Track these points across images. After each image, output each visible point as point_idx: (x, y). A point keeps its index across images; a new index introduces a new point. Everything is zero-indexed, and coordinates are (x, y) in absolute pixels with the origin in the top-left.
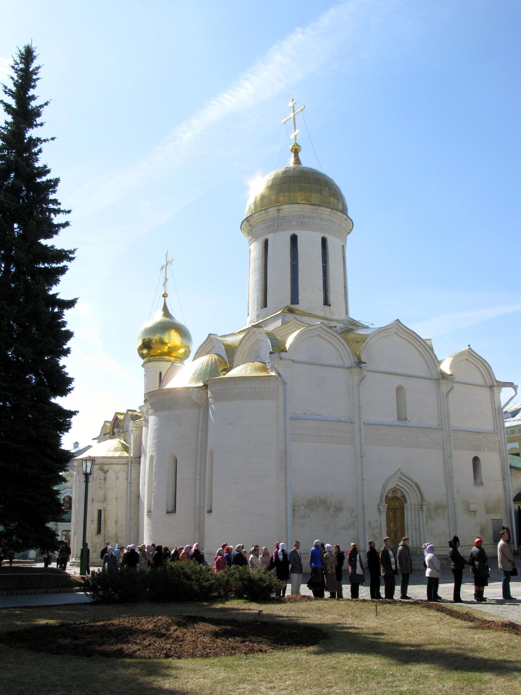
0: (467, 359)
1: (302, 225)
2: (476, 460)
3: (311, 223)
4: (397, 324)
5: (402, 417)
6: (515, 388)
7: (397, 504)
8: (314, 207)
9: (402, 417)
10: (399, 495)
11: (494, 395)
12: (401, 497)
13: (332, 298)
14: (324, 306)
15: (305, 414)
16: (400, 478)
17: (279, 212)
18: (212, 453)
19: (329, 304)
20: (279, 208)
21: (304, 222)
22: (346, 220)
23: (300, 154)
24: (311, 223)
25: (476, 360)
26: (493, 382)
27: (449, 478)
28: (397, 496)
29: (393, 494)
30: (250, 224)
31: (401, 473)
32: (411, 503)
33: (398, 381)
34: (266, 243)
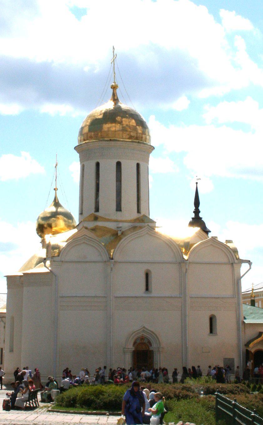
4: (148, 227)
7: (144, 347)
10: (146, 341)
14: (116, 212)
28: (144, 342)
29: (141, 340)
31: (144, 327)
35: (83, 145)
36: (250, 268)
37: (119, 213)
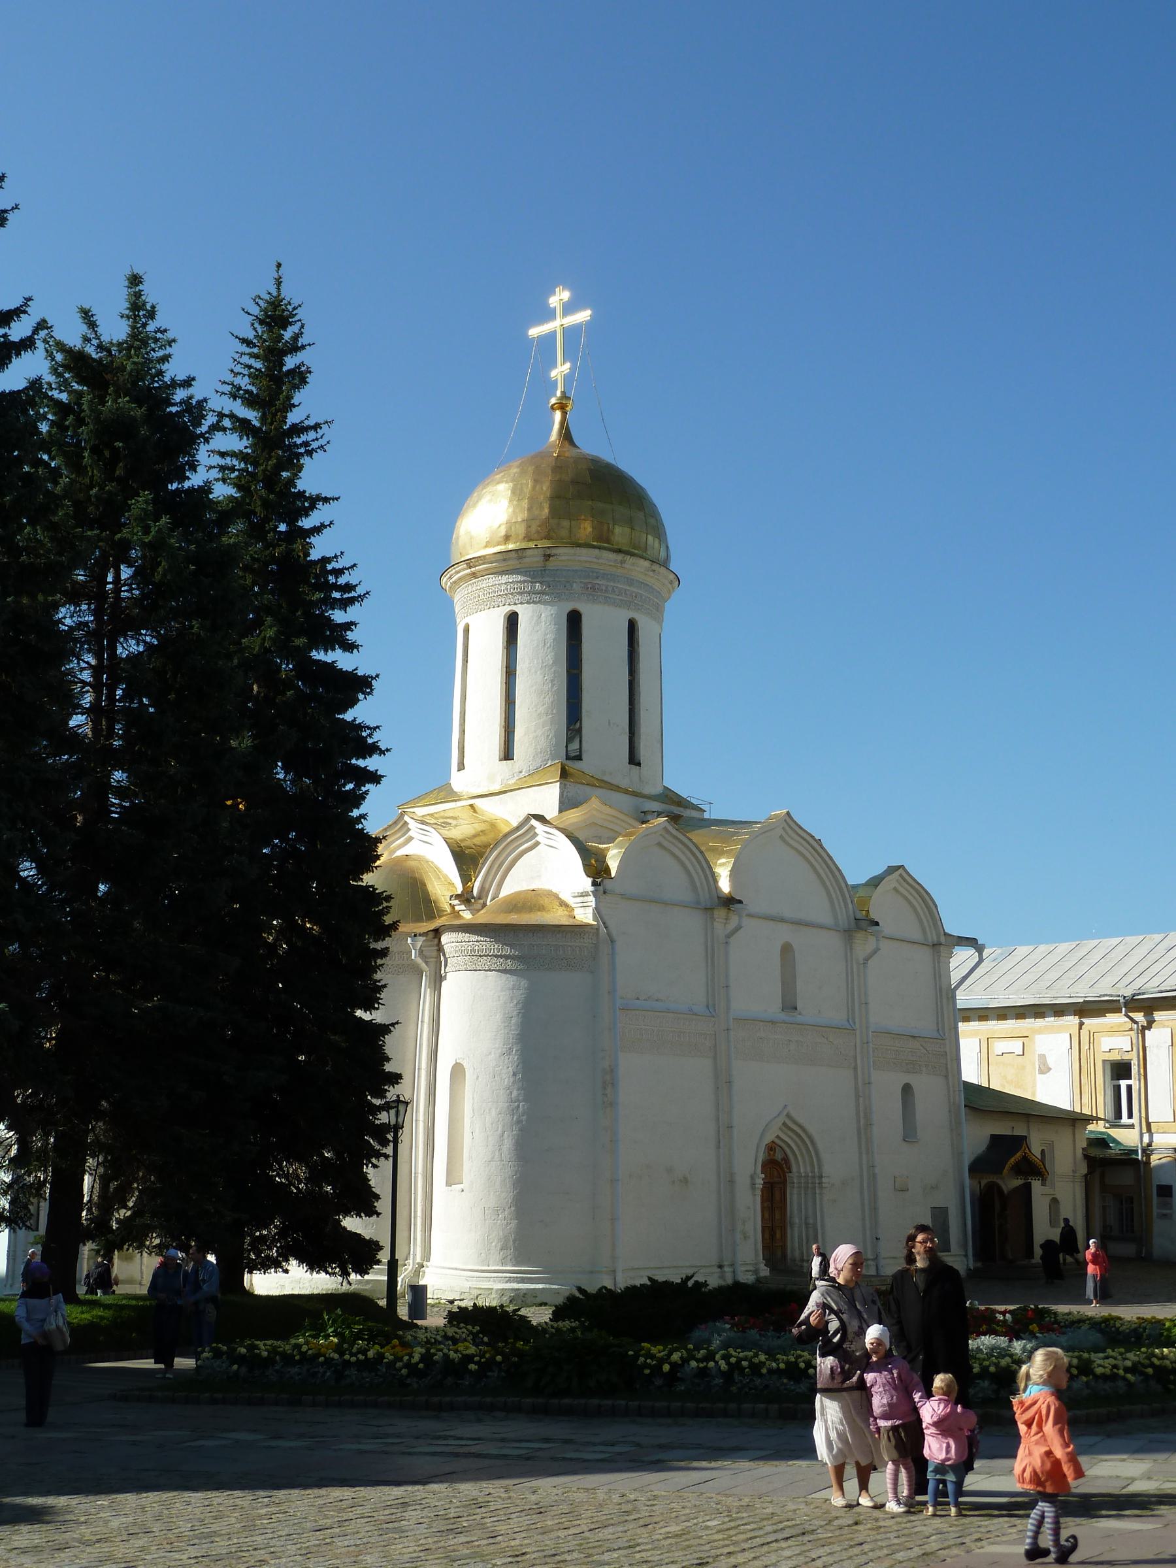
0: (895, 889)
1: (593, 592)
2: (907, 1089)
3: (610, 589)
5: (790, 1006)
6: (980, 949)
7: (776, 1173)
8: (620, 557)
9: (790, 1006)
10: (779, 1156)
11: (939, 962)
12: (782, 1160)
15: (638, 999)
16: (784, 1124)
17: (546, 560)
19: (637, 761)
20: (548, 552)
21: (597, 587)
22: (671, 583)
24: (610, 589)
25: (911, 890)
26: (938, 936)
27: (864, 1125)
28: (776, 1158)
30: (474, 573)
31: (788, 1116)
32: (799, 1172)
33: (784, 934)
35: (529, 552)
36: (981, 960)
37: (635, 768)
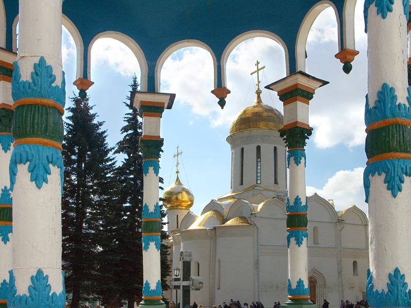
13: (279, 181)
18: (219, 261)
23: (261, 95)
34: (243, 149)
